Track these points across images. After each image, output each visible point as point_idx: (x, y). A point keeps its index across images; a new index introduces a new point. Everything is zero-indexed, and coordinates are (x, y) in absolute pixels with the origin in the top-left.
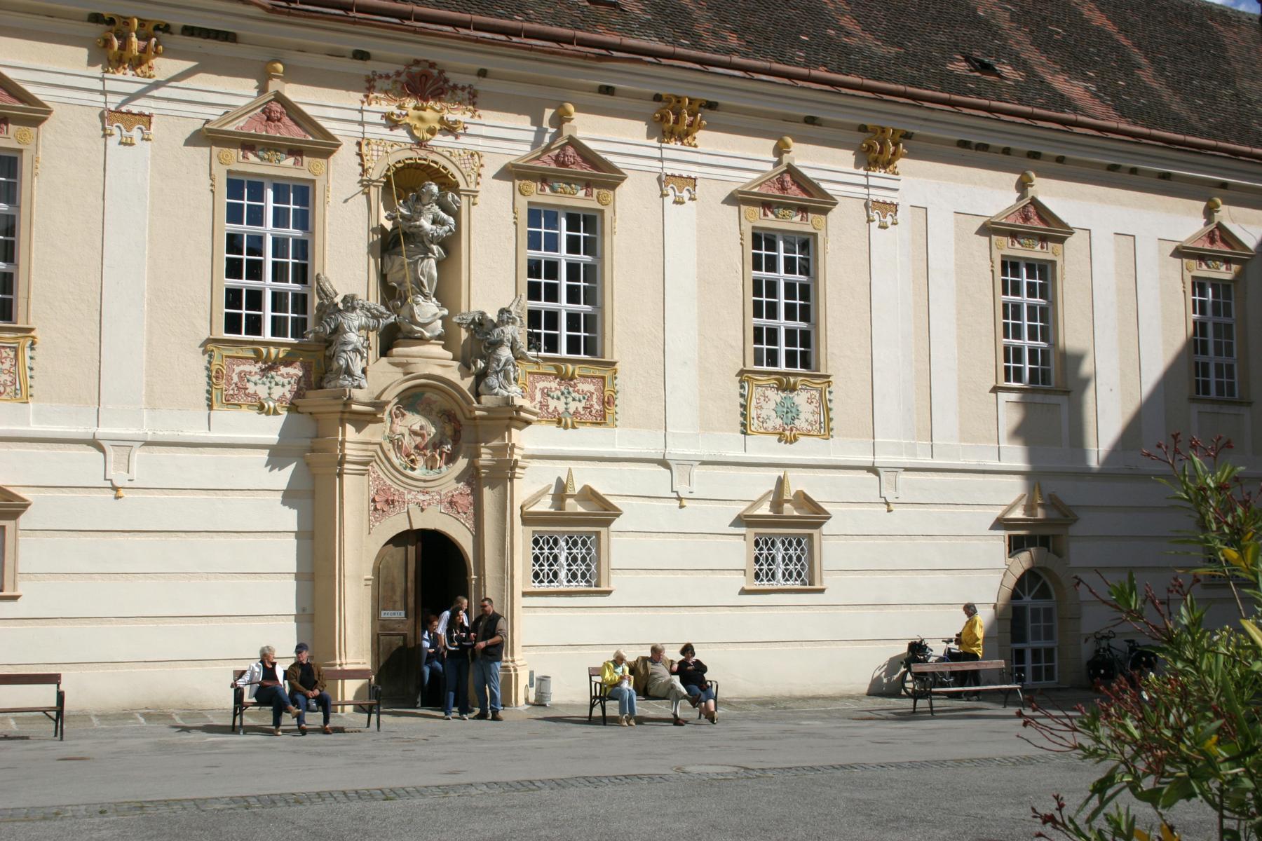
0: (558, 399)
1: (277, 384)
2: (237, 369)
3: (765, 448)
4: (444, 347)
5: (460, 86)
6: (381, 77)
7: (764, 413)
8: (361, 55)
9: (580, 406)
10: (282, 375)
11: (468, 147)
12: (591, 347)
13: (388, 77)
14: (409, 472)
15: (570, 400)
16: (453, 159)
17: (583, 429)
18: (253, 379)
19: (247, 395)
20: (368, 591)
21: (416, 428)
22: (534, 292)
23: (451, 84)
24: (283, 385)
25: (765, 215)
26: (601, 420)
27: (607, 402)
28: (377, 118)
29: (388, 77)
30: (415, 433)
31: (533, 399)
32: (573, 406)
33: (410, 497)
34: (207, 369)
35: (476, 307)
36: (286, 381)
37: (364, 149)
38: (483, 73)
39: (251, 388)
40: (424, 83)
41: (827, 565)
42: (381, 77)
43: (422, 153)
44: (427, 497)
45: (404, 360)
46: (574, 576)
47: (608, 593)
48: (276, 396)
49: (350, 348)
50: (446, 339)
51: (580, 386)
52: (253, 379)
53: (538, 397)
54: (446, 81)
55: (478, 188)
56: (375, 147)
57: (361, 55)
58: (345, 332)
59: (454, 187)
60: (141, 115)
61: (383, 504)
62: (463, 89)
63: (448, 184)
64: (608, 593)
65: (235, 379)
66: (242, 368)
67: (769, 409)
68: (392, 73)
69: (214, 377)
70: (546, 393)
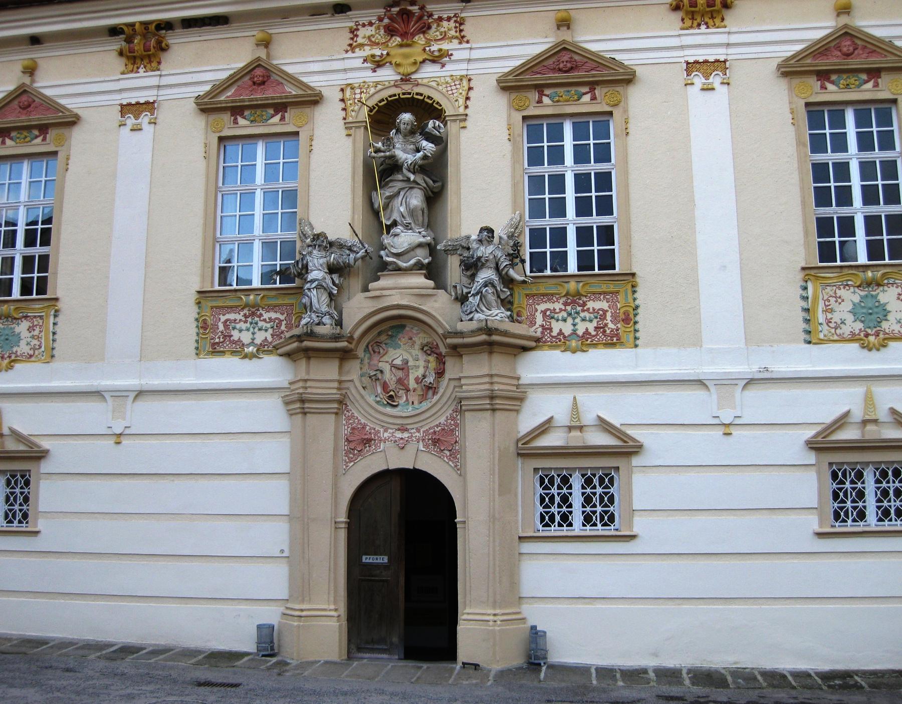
0: (565, 320)
1: (260, 330)
2: (223, 318)
3: (846, 359)
4: (427, 278)
7: (836, 317)
9: (591, 327)
10: (265, 320)
11: (454, 73)
12: (608, 260)
14: (389, 410)
15: (578, 320)
16: (440, 88)
17: (593, 353)
18: (238, 326)
20: (343, 534)
21: (398, 362)
23: (436, 17)
24: (266, 330)
25: (823, 87)
26: (613, 341)
27: (629, 318)
28: (358, 63)
29: (371, 24)
30: (398, 368)
31: (533, 323)
32: (581, 329)
33: (386, 435)
34: (197, 320)
35: (464, 233)
36: (269, 325)
37: (348, 93)
39: (236, 335)
41: (42, 508)
42: (364, 25)
43: (407, 88)
44: (406, 435)
45: (377, 293)
46: (886, 513)
47: (633, 537)
48: (258, 341)
49: (314, 285)
50: (433, 271)
51: (591, 305)
53: (539, 320)
54: (430, 15)
55: (468, 111)
56: (358, 91)
58: (312, 271)
59: (436, 112)
60: (147, 103)
61: (361, 442)
62: (449, 19)
64: (633, 537)
65: (221, 327)
66: (228, 316)
67: (843, 312)
69: (203, 326)
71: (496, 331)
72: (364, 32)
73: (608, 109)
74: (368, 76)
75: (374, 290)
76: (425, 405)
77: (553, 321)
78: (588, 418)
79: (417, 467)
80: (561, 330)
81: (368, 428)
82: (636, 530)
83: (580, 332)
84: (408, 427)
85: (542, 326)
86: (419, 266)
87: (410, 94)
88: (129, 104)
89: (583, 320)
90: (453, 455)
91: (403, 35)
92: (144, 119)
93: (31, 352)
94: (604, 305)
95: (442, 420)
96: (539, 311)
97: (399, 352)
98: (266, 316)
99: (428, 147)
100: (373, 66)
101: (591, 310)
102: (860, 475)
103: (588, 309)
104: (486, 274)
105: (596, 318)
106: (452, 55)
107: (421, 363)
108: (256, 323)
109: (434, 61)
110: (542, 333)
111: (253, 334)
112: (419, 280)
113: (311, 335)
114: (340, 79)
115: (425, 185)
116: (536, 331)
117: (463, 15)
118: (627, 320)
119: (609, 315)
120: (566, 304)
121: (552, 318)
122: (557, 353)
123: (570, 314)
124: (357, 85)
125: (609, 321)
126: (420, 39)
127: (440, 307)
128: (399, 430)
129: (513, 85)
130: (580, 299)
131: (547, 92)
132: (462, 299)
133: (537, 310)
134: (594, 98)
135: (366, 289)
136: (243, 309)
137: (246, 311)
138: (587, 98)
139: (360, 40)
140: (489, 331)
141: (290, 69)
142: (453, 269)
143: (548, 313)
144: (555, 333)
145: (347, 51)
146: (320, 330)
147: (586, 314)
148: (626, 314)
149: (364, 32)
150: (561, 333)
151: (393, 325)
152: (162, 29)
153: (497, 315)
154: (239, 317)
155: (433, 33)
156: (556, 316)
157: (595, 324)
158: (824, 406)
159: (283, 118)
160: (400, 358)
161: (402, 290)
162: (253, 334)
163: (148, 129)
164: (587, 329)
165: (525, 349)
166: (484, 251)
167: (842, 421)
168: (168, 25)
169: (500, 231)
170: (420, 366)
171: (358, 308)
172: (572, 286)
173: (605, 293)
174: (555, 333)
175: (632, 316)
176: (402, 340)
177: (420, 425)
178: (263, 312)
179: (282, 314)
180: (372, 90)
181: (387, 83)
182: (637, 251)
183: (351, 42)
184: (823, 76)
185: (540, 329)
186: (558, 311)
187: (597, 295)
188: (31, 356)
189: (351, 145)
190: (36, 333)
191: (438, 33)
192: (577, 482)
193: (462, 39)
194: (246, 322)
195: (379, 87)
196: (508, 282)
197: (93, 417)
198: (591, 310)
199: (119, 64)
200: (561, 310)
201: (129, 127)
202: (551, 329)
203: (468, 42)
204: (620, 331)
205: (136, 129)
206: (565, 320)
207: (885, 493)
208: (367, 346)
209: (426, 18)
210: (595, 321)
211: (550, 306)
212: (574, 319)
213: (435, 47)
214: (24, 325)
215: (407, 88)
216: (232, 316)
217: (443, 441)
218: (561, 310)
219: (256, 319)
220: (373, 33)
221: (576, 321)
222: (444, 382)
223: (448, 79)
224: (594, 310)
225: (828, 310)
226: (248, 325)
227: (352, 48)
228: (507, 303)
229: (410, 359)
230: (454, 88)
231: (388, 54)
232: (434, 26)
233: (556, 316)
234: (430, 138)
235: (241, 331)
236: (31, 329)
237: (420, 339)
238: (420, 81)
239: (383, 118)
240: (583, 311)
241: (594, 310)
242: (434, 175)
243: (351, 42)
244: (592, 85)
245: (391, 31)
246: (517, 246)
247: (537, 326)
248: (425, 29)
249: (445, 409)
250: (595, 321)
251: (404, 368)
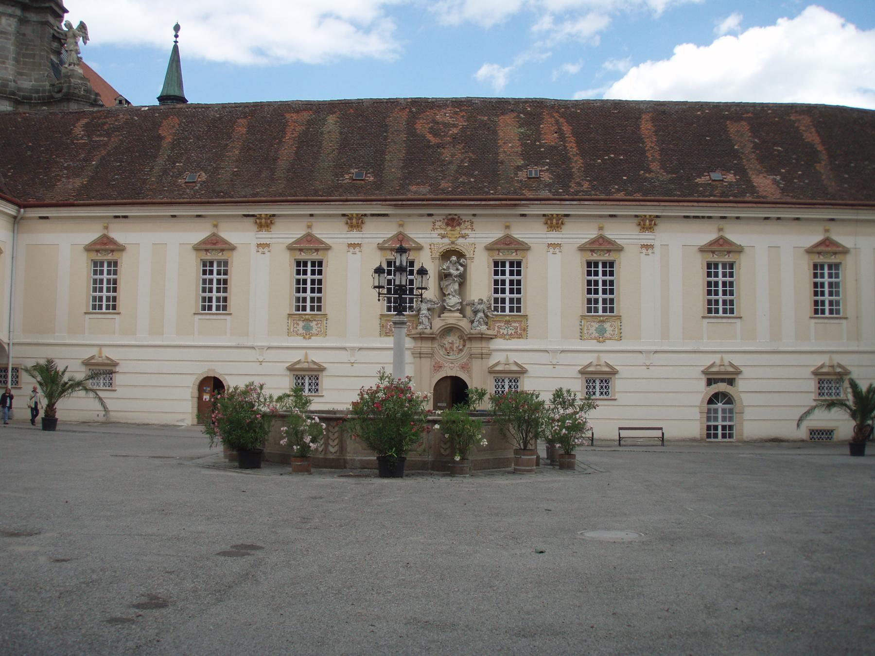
7: (590, 332)
8: (430, 215)
22: (496, 291)
26: (520, 337)
28: (436, 236)
35: (472, 298)
38: (474, 215)
40: (453, 222)
50: (461, 311)
57: (430, 215)
61: (438, 367)
63: (460, 255)
67: (592, 330)
69: (382, 326)
70: (499, 328)
72: (438, 224)
74: (439, 240)
76: (460, 355)
78: (511, 361)
86: (458, 310)
90: (468, 372)
91: (452, 226)
92: (357, 250)
99: (461, 269)
102: (594, 381)
104: (480, 315)
109: (463, 237)
112: (458, 314)
113: (424, 333)
114: (429, 241)
118: (524, 330)
126: (458, 228)
127: (464, 324)
129: (489, 248)
132: (472, 322)
135: (439, 317)
140: (482, 334)
141: (411, 236)
142: (469, 311)
146: (426, 331)
149: (438, 224)
151: (448, 330)
153: (483, 328)
155: (463, 226)
158: (584, 360)
161: (452, 318)
163: (359, 254)
166: (480, 307)
167: (590, 365)
168: (365, 215)
169: (485, 300)
170: (458, 343)
171: (438, 324)
172: (507, 318)
176: (452, 334)
182: (528, 307)
184: (592, 251)
187: (515, 322)
192: (507, 381)
196: (487, 316)
197: (343, 356)
199: (346, 228)
204: (522, 333)
205: (354, 253)
207: (602, 387)
213: (463, 232)
214: (314, 323)
222: (465, 349)
225: (588, 329)
227: (434, 229)
228: (487, 324)
234: (462, 265)
236: (317, 324)
237: (458, 334)
239: (446, 255)
242: (462, 280)
244: (516, 250)
245: (448, 224)
246: (490, 304)
248: (459, 224)
251: (452, 343)
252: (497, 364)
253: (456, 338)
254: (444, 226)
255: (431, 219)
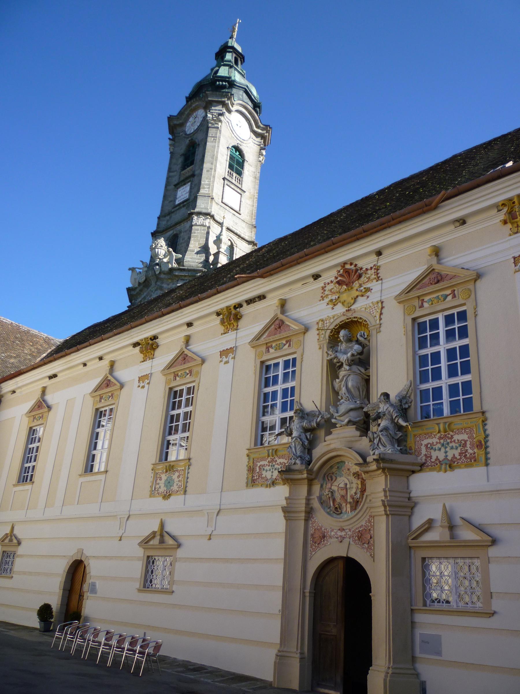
2: (259, 464)
5: (369, 268)
6: (328, 284)
8: (316, 277)
9: (457, 453)
10: (278, 464)
12: (468, 404)
13: (332, 282)
15: (448, 449)
19: (262, 478)
23: (364, 269)
26: (471, 461)
27: (483, 445)
38: (379, 253)
42: (328, 284)
44: (343, 533)
52: (265, 468)
55: (381, 322)
57: (316, 277)
62: (371, 268)
64: (494, 613)
65: (258, 470)
68: (333, 279)
71: (391, 461)
72: (328, 287)
73: (463, 302)
75: (328, 440)
77: (432, 451)
79: (350, 555)
80: (437, 457)
81: (323, 529)
82: (494, 608)
83: (449, 458)
84: (345, 528)
85: (426, 455)
87: (350, 318)
88: (224, 350)
89: (452, 448)
93: (178, 489)
94: (465, 437)
95: (363, 523)
96: (423, 445)
97: (343, 478)
98: (279, 461)
100: (332, 306)
101: (456, 441)
103: (454, 441)
105: (460, 446)
106: (372, 289)
107: (354, 486)
108: (274, 466)
109: (362, 296)
110: (426, 460)
111: (272, 472)
115: (359, 372)
116: (422, 459)
117: (379, 264)
118: (479, 445)
119: (468, 443)
120: (440, 438)
121: (432, 448)
122: (434, 473)
123: (443, 445)
124: (324, 319)
125: (468, 448)
128: (339, 530)
130: (449, 434)
131: (426, 298)
133: (422, 445)
134: (454, 296)
136: (267, 459)
137: (269, 459)
138: (450, 298)
139: (326, 293)
143: (429, 446)
144: (433, 460)
145: (320, 300)
147: (453, 444)
148: (480, 442)
150: (437, 459)
152: (238, 308)
154: (266, 463)
155: (363, 279)
156: (434, 447)
157: (459, 450)
159: (289, 345)
160: (343, 483)
162: (272, 472)
164: (454, 455)
165: (413, 472)
168: (240, 305)
173: (465, 429)
174: (433, 460)
175: (483, 442)
177: (351, 526)
178: (277, 459)
179: (286, 459)
180: (332, 320)
181: (339, 314)
183: (322, 295)
185: (424, 458)
186: (435, 444)
188: (178, 491)
189: (321, 353)
190: (180, 479)
191: (365, 278)
193: (378, 279)
194: (269, 466)
195: (336, 318)
198: (456, 441)
200: (437, 443)
201: (223, 362)
202: (431, 457)
203: (381, 279)
204: (479, 453)
206: (440, 449)
208: (324, 476)
209: (359, 271)
210: (459, 448)
211: (430, 441)
212: (446, 448)
215: (349, 315)
216: (262, 463)
217: (364, 537)
218: (437, 443)
219: (274, 463)
220: (333, 287)
221: (447, 449)
223: (371, 305)
224: (458, 440)
226: (270, 467)
227: (323, 298)
229: (348, 483)
230: (374, 309)
231: (338, 297)
232: (364, 275)
233: (434, 447)
235: (267, 471)
236: (179, 477)
238: (356, 309)
240: (451, 442)
241: (458, 440)
243: (322, 295)
247: (422, 455)
249: (365, 515)
250: (459, 448)
252: (429, 525)
253: (352, 478)
254: (337, 287)
255: (320, 283)
